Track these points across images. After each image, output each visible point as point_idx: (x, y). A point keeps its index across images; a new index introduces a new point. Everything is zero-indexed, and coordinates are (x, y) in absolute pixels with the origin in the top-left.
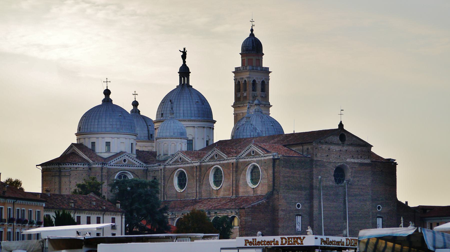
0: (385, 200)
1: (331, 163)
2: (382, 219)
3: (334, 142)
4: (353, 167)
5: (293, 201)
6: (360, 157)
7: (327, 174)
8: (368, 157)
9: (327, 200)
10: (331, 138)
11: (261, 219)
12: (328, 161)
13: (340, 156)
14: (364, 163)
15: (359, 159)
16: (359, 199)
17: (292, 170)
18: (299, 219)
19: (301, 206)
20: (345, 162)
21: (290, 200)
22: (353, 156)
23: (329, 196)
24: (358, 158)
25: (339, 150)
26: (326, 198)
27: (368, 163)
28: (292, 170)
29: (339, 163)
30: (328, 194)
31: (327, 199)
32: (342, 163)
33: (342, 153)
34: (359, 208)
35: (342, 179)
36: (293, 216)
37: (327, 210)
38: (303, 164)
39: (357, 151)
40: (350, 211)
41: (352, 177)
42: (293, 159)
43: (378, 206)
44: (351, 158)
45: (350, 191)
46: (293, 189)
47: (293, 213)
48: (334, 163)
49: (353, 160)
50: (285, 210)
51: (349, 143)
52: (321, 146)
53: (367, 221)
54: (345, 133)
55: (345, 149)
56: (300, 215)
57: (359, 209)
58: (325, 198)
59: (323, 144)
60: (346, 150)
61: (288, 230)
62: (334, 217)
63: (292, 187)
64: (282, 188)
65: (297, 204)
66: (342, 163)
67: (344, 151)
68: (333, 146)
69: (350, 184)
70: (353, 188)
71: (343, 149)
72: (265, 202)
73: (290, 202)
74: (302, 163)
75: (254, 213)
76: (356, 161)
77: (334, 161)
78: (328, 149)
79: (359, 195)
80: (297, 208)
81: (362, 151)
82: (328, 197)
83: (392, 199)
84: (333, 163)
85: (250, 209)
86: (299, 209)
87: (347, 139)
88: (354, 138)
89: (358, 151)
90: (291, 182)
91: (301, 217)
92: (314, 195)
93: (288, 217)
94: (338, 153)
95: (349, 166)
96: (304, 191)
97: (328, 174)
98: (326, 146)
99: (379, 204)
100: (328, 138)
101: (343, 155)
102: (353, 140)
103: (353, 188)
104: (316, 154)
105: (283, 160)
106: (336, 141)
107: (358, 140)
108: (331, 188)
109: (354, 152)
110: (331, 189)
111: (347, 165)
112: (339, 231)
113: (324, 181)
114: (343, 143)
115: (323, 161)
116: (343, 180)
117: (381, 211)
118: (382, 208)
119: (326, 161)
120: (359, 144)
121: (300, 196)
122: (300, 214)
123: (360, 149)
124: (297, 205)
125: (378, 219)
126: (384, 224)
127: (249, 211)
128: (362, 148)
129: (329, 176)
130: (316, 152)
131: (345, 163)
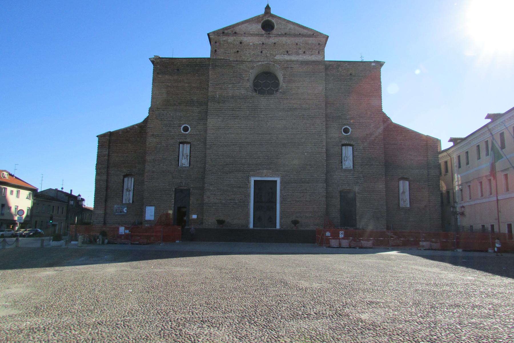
0: (359, 118)
1: (245, 62)
2: (353, 149)
3: (251, 33)
4: (288, 68)
5: (175, 122)
6: (301, 52)
7: (236, 79)
8: (317, 52)
9: (234, 117)
10: (246, 27)
11: (129, 152)
12: (238, 59)
13: (263, 52)
14: (310, 61)
15: (300, 56)
16: (300, 115)
17: (176, 77)
18: (186, 149)
19: (190, 129)
20: (272, 60)
21: (169, 121)
22: (287, 52)
23: (238, 111)
24: (297, 54)
25: (260, 44)
26: (232, 114)
27: (318, 61)
28: (176, 77)
29: (259, 61)
30: (237, 109)
31: (234, 115)
32: (266, 62)
33: (266, 47)
34: (299, 129)
35: (276, 89)
36: (174, 144)
37: (233, 132)
38: (197, 67)
39: (297, 44)
40: (281, 134)
41: (285, 82)
42: (179, 62)
43: (343, 128)
44: (284, 55)
45: (281, 103)
46: (175, 105)
47: (173, 139)
48: (250, 62)
49: (287, 57)
50: (160, 136)
51: (280, 33)
52: (225, 39)
53: (315, 150)
54: (273, 19)
55: (273, 41)
56: (187, 143)
57: (298, 131)
58: (231, 113)
59: (229, 36)
60: (275, 43)
61: (163, 165)
62: (247, 142)
63: (174, 101)
64: (156, 103)
65: (183, 126)
66: (266, 62)
67: (270, 45)
68: (249, 38)
69: (281, 92)
70: (287, 99)
71: (269, 42)
72: (136, 127)
73: (170, 123)
74: (196, 66)
75: (117, 144)
76: (294, 58)
77: (250, 59)
78: (239, 42)
79: (300, 109)
80: (182, 132)
81: (307, 44)
82: (237, 112)
83: (372, 116)
84: (248, 62)
85: (107, 138)
86: (187, 134)
87: (276, 27)
88: (291, 26)
89: (299, 43)
90: (173, 94)
91: (189, 146)
92: (210, 111)
93: (165, 145)
94: (258, 48)
95: (279, 66)
96: (198, 107)
97: (237, 78)
98: (235, 38)
99: (345, 125)
100: (240, 26)
101: (268, 51)
102: (289, 28)
103: (287, 99)
104: (216, 51)
105: (160, 64)
106: (254, 30)
107: (297, 28)
108: (242, 99)
109: (289, 44)
110: (243, 100)
111: (275, 65)
112: (257, 165)
113: (230, 89)
114: (269, 32)
115: (229, 60)
116: (277, 91)
117: (350, 135)
118: (351, 131)
119: (235, 60)
120: (300, 34)
121: (188, 114)
122: (188, 140)
123: (302, 41)
124: (182, 128)
125: (344, 148)
126: (357, 156)
127: (104, 140)
128: (306, 39)
129: (239, 81)
130: (216, 47)
131: (272, 62)
